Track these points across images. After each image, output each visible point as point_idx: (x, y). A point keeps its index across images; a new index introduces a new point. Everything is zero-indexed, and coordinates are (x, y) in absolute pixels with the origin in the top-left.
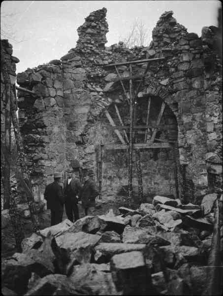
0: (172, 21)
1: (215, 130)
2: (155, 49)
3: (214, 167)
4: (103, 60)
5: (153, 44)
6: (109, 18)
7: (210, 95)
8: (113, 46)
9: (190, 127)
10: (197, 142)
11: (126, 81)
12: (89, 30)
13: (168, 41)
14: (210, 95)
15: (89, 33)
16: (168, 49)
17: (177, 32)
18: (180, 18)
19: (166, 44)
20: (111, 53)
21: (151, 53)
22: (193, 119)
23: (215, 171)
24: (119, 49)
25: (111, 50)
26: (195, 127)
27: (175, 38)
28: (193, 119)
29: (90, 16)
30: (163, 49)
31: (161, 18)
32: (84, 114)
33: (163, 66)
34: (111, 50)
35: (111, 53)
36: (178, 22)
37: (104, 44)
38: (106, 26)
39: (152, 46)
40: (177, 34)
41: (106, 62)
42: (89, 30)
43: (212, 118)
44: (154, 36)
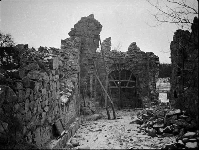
0: (136, 46)
1: (151, 85)
2: (128, 54)
3: (153, 96)
4: (110, 56)
5: (128, 52)
6: (112, 40)
7: (151, 74)
8: (113, 51)
9: (141, 82)
10: (144, 87)
11: (118, 64)
12: (106, 45)
13: (134, 52)
14: (151, 74)
15: (106, 46)
16: (134, 55)
17: (138, 50)
18: (138, 45)
19: (133, 53)
20: (112, 53)
21: (127, 55)
22: (143, 80)
23: (153, 97)
24: (115, 52)
25: (112, 52)
26: (143, 82)
27: (136, 52)
28: (143, 80)
29: (106, 40)
30: (132, 55)
31: (131, 44)
32: (104, 75)
33: (131, 60)
34: (112, 52)
35: (112, 53)
36: (138, 46)
37: (110, 50)
38: (111, 44)
39: (128, 53)
40: (137, 50)
41: (111, 57)
42: (106, 45)
43: (151, 81)
44: (128, 50)
